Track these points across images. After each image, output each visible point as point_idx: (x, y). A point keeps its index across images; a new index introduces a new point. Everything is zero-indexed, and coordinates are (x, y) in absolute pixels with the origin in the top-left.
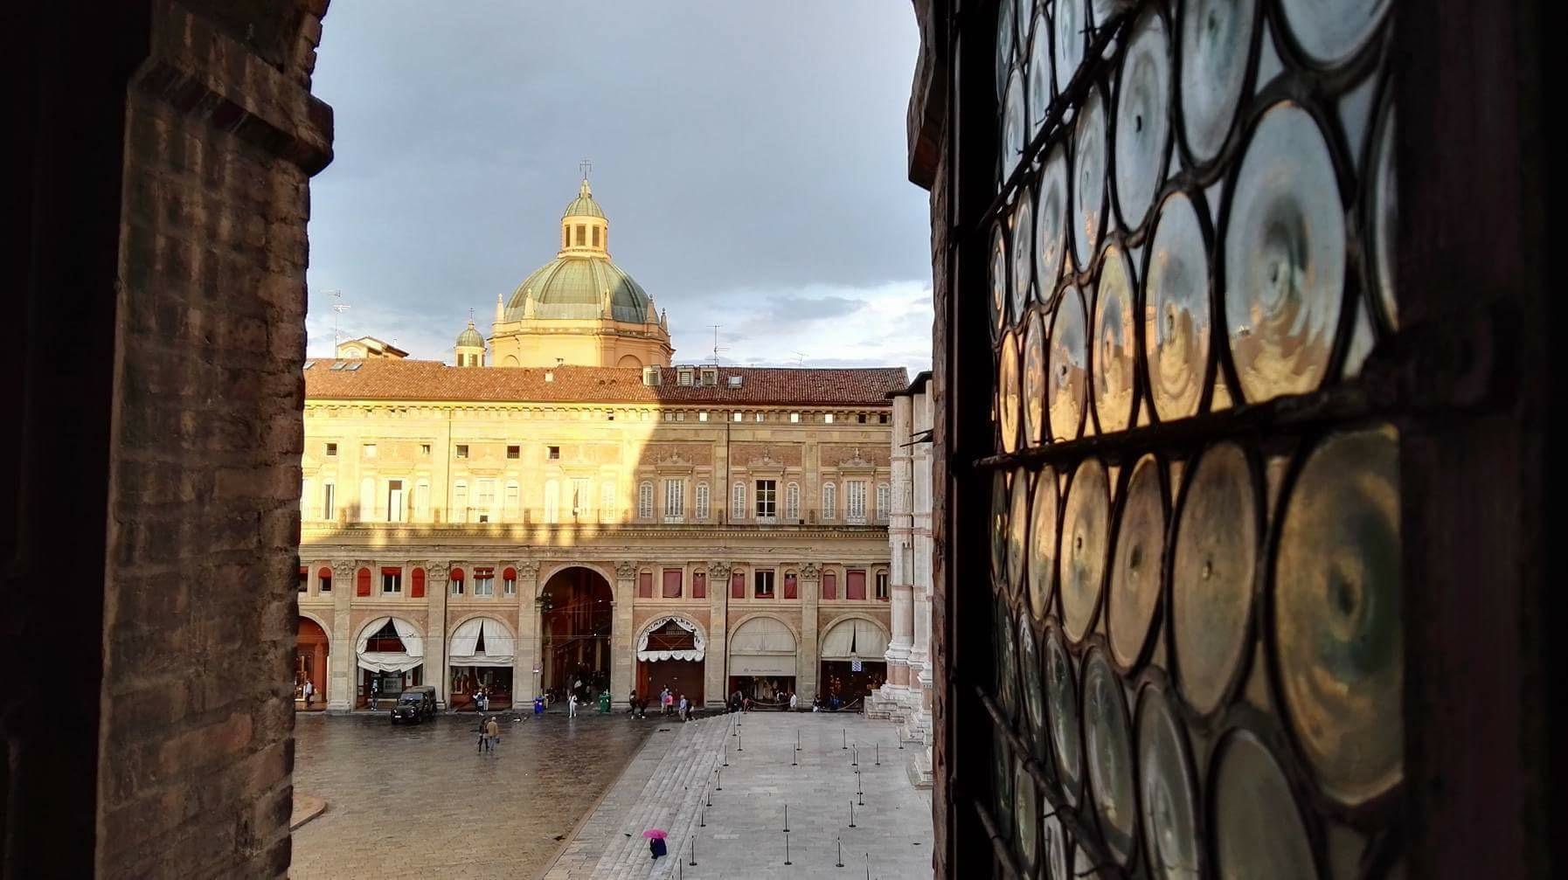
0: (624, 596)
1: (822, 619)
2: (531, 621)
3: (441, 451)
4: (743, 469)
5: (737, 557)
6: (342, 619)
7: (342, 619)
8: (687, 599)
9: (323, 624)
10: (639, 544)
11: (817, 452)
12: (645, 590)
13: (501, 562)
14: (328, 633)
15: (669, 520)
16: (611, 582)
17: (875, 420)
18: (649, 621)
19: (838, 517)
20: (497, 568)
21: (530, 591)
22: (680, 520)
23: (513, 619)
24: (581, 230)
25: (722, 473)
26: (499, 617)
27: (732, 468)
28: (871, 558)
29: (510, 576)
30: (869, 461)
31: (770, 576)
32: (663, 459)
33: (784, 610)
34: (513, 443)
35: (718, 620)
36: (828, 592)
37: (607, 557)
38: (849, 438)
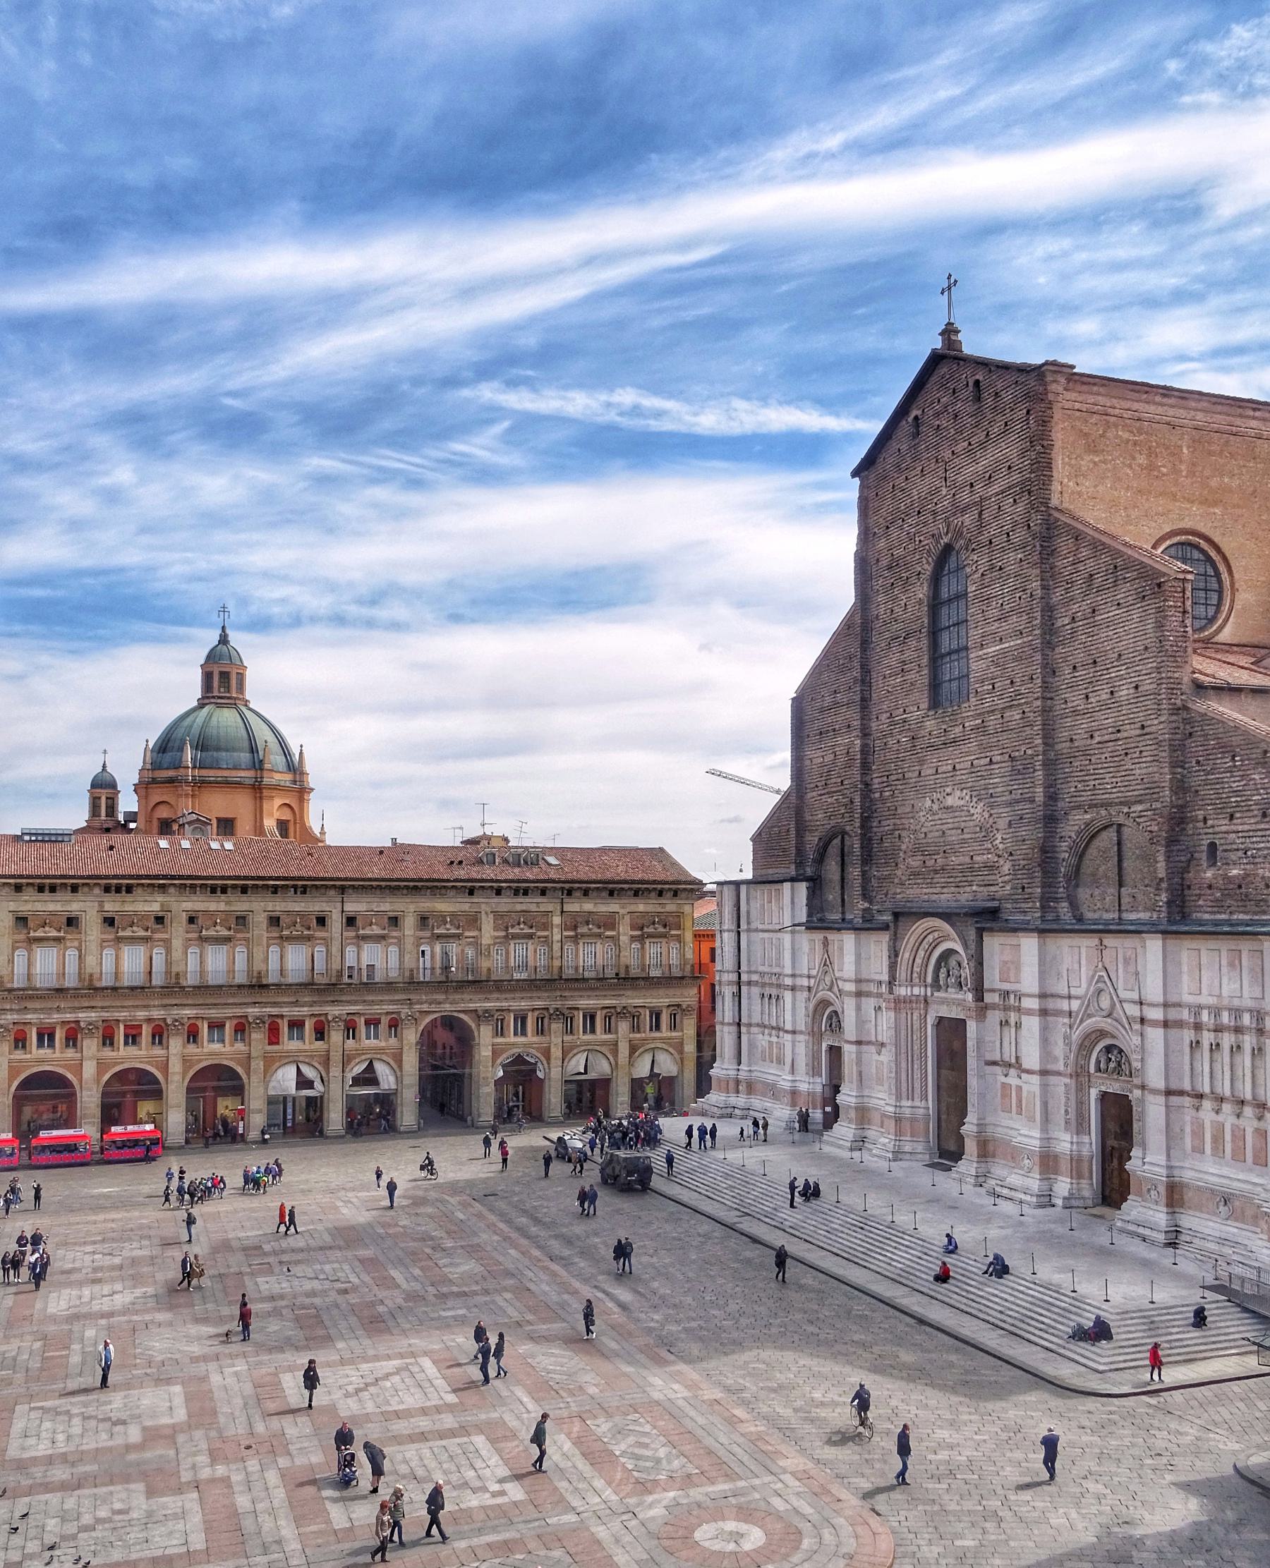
0: (485, 1038)
1: (633, 1049)
2: (411, 1061)
3: (336, 922)
4: (572, 933)
5: (571, 1003)
6: (258, 1065)
7: (258, 1065)
8: (531, 1038)
9: (239, 1070)
10: (495, 995)
11: (627, 918)
12: (500, 1031)
13: (387, 1013)
14: (244, 1076)
15: (517, 976)
16: (473, 1026)
17: (670, 894)
18: (505, 1056)
19: (643, 970)
20: (383, 1018)
21: (411, 1036)
22: (524, 976)
23: (398, 1059)
24: (225, 676)
25: (557, 937)
26: (384, 1057)
27: (565, 933)
28: (667, 1001)
29: (394, 1024)
30: (665, 926)
31: (593, 1017)
32: (513, 926)
33: (604, 1043)
34: (391, 914)
35: (556, 1053)
36: (636, 1028)
37: (472, 1006)
38: (650, 908)
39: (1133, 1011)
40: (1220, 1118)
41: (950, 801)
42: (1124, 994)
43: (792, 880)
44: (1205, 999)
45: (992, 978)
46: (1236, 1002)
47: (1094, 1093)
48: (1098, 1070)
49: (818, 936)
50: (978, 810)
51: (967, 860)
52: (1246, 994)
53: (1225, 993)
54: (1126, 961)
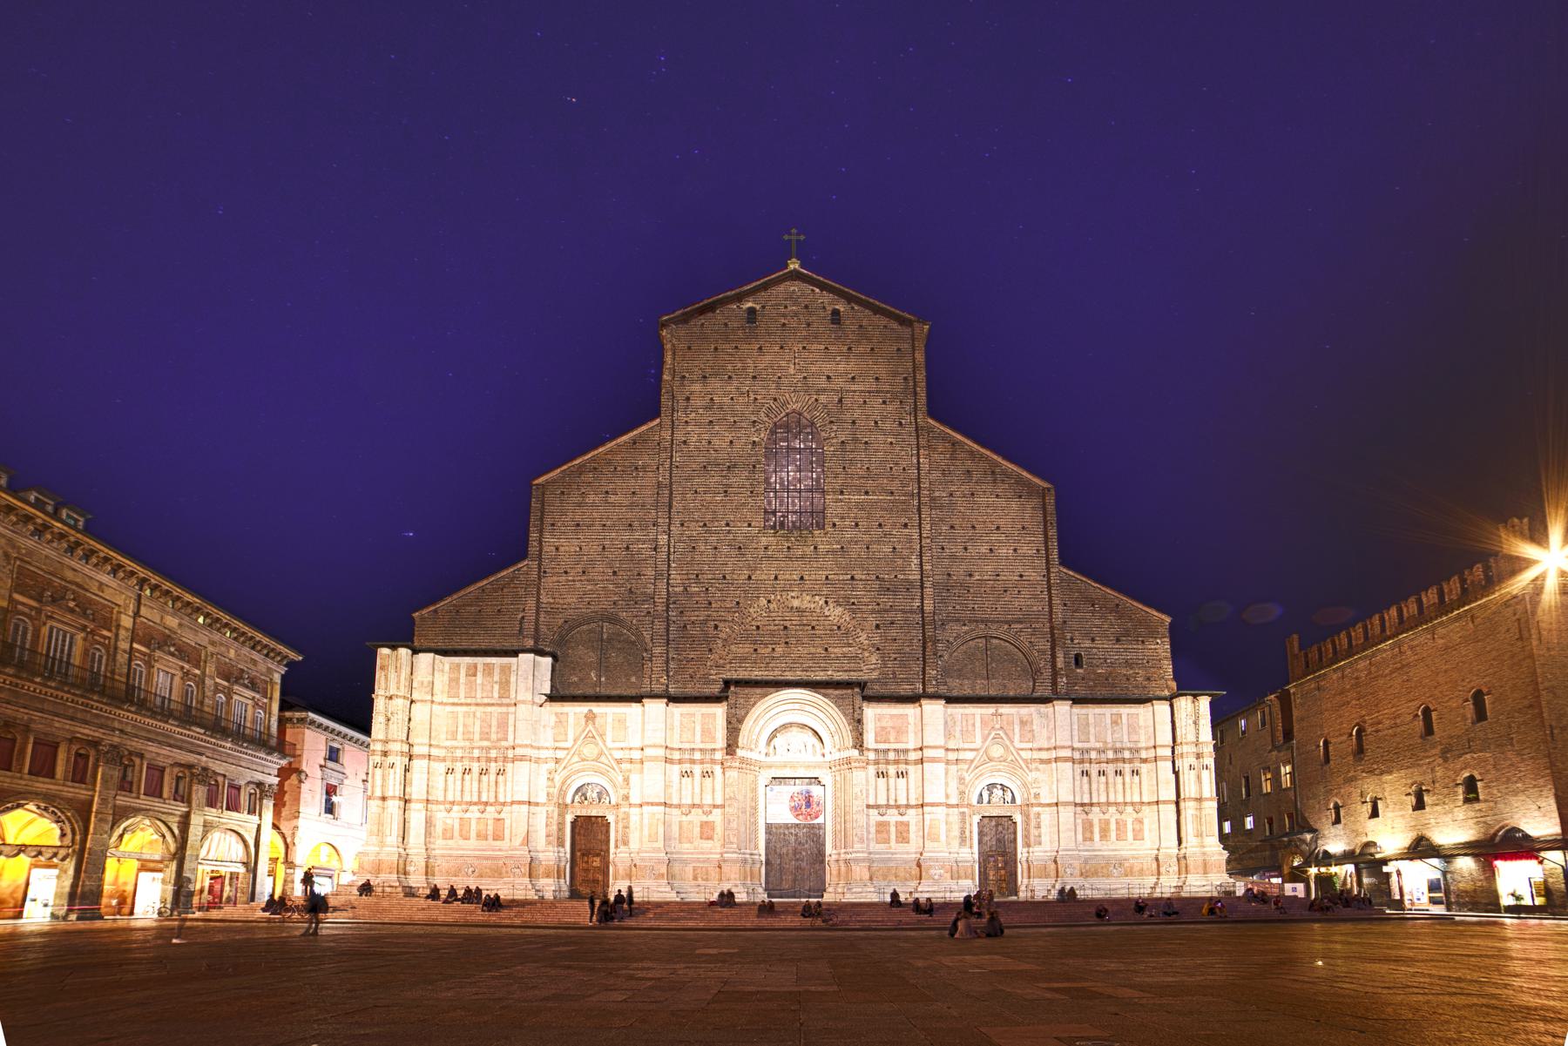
39: (1037, 755)
40: (1107, 816)
41: (796, 603)
42: (1018, 744)
43: (540, 652)
44: (1093, 744)
45: (870, 740)
46: (1118, 745)
47: (976, 819)
48: (980, 800)
49: (575, 711)
50: (835, 613)
51: (820, 650)
52: (1126, 739)
53: (1109, 739)
54: (1023, 723)
